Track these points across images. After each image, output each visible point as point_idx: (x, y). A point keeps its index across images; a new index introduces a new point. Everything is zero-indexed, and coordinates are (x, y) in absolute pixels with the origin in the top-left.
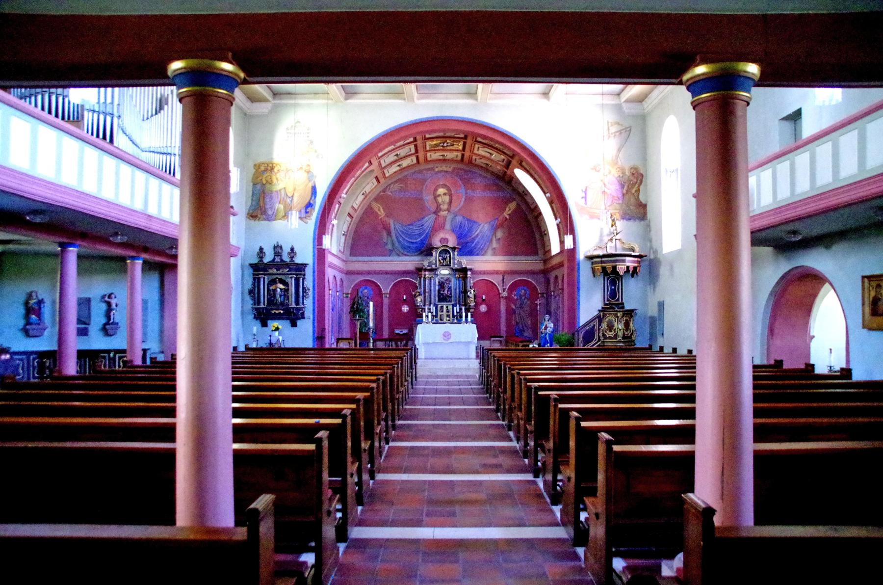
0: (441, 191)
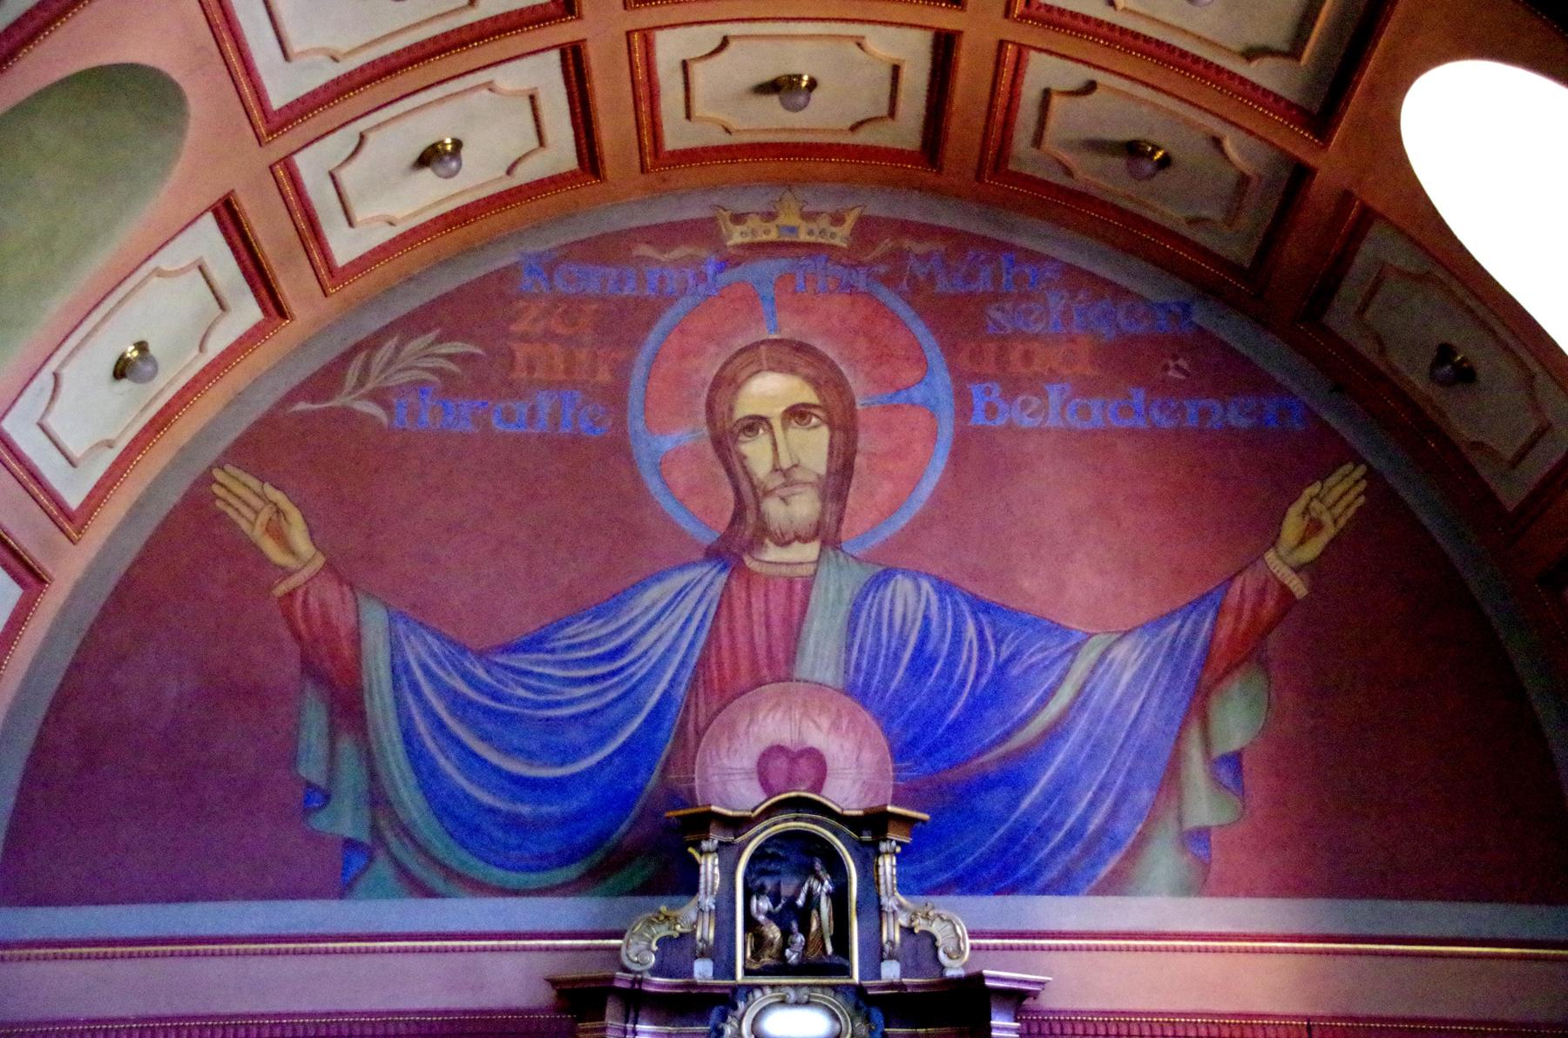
0: (769, 391)
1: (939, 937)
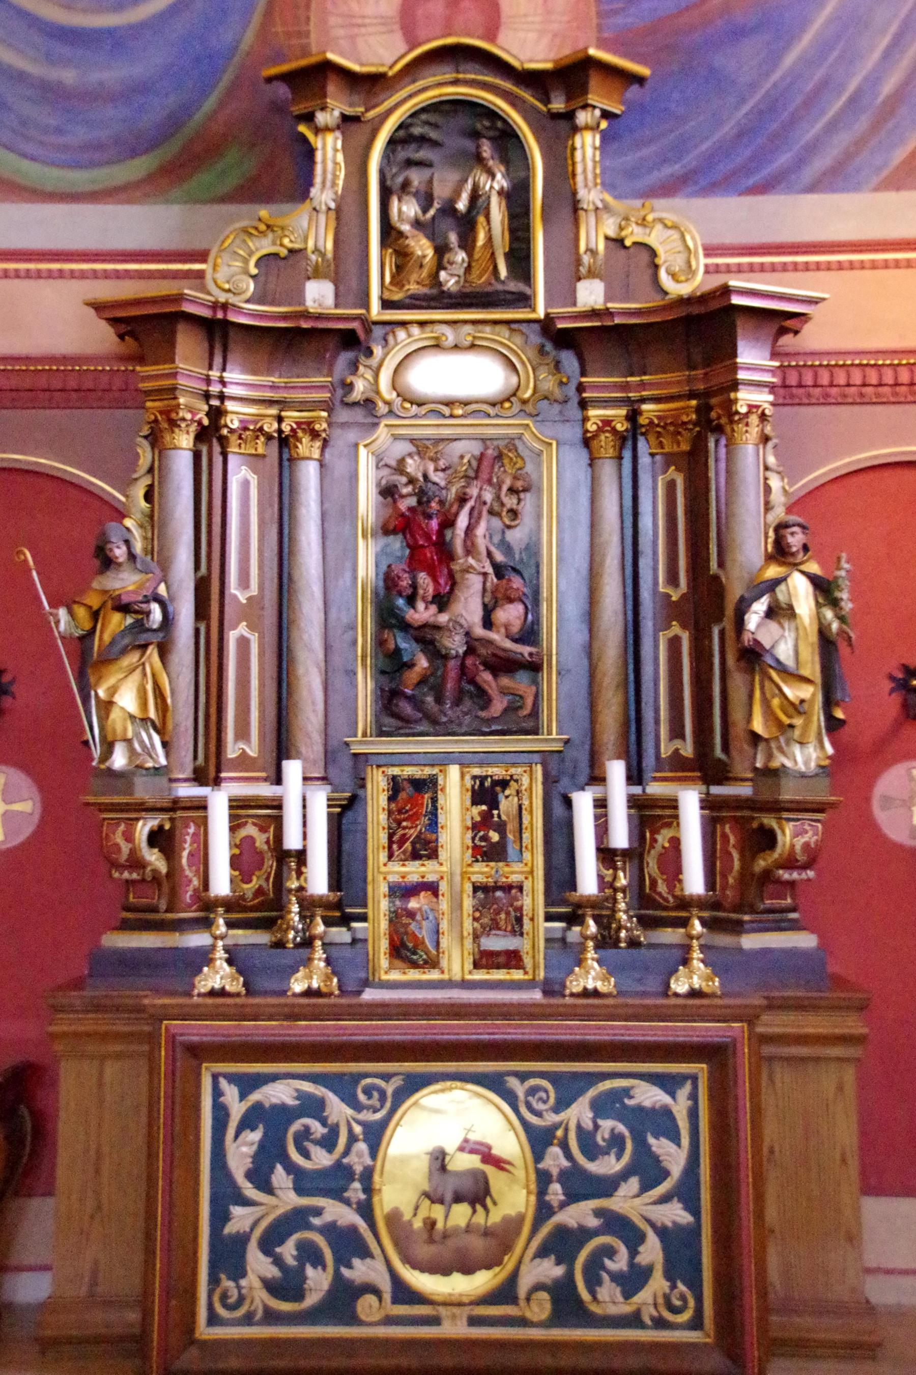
1: (660, 250)
